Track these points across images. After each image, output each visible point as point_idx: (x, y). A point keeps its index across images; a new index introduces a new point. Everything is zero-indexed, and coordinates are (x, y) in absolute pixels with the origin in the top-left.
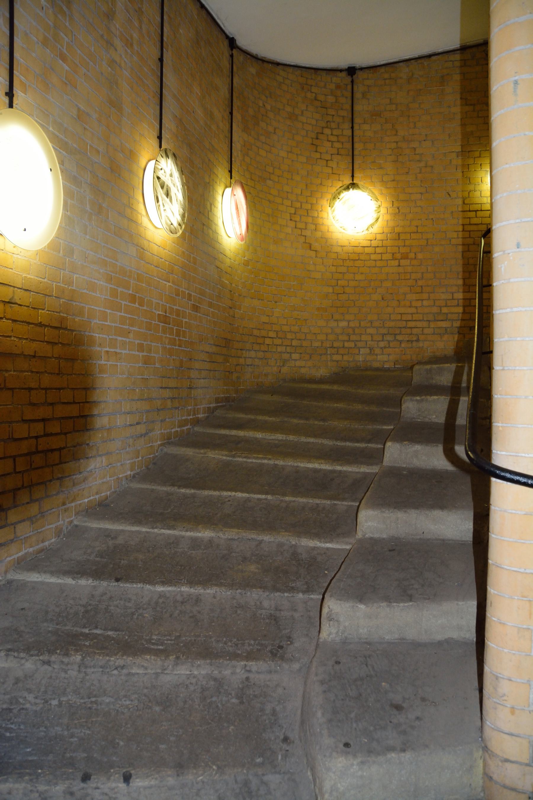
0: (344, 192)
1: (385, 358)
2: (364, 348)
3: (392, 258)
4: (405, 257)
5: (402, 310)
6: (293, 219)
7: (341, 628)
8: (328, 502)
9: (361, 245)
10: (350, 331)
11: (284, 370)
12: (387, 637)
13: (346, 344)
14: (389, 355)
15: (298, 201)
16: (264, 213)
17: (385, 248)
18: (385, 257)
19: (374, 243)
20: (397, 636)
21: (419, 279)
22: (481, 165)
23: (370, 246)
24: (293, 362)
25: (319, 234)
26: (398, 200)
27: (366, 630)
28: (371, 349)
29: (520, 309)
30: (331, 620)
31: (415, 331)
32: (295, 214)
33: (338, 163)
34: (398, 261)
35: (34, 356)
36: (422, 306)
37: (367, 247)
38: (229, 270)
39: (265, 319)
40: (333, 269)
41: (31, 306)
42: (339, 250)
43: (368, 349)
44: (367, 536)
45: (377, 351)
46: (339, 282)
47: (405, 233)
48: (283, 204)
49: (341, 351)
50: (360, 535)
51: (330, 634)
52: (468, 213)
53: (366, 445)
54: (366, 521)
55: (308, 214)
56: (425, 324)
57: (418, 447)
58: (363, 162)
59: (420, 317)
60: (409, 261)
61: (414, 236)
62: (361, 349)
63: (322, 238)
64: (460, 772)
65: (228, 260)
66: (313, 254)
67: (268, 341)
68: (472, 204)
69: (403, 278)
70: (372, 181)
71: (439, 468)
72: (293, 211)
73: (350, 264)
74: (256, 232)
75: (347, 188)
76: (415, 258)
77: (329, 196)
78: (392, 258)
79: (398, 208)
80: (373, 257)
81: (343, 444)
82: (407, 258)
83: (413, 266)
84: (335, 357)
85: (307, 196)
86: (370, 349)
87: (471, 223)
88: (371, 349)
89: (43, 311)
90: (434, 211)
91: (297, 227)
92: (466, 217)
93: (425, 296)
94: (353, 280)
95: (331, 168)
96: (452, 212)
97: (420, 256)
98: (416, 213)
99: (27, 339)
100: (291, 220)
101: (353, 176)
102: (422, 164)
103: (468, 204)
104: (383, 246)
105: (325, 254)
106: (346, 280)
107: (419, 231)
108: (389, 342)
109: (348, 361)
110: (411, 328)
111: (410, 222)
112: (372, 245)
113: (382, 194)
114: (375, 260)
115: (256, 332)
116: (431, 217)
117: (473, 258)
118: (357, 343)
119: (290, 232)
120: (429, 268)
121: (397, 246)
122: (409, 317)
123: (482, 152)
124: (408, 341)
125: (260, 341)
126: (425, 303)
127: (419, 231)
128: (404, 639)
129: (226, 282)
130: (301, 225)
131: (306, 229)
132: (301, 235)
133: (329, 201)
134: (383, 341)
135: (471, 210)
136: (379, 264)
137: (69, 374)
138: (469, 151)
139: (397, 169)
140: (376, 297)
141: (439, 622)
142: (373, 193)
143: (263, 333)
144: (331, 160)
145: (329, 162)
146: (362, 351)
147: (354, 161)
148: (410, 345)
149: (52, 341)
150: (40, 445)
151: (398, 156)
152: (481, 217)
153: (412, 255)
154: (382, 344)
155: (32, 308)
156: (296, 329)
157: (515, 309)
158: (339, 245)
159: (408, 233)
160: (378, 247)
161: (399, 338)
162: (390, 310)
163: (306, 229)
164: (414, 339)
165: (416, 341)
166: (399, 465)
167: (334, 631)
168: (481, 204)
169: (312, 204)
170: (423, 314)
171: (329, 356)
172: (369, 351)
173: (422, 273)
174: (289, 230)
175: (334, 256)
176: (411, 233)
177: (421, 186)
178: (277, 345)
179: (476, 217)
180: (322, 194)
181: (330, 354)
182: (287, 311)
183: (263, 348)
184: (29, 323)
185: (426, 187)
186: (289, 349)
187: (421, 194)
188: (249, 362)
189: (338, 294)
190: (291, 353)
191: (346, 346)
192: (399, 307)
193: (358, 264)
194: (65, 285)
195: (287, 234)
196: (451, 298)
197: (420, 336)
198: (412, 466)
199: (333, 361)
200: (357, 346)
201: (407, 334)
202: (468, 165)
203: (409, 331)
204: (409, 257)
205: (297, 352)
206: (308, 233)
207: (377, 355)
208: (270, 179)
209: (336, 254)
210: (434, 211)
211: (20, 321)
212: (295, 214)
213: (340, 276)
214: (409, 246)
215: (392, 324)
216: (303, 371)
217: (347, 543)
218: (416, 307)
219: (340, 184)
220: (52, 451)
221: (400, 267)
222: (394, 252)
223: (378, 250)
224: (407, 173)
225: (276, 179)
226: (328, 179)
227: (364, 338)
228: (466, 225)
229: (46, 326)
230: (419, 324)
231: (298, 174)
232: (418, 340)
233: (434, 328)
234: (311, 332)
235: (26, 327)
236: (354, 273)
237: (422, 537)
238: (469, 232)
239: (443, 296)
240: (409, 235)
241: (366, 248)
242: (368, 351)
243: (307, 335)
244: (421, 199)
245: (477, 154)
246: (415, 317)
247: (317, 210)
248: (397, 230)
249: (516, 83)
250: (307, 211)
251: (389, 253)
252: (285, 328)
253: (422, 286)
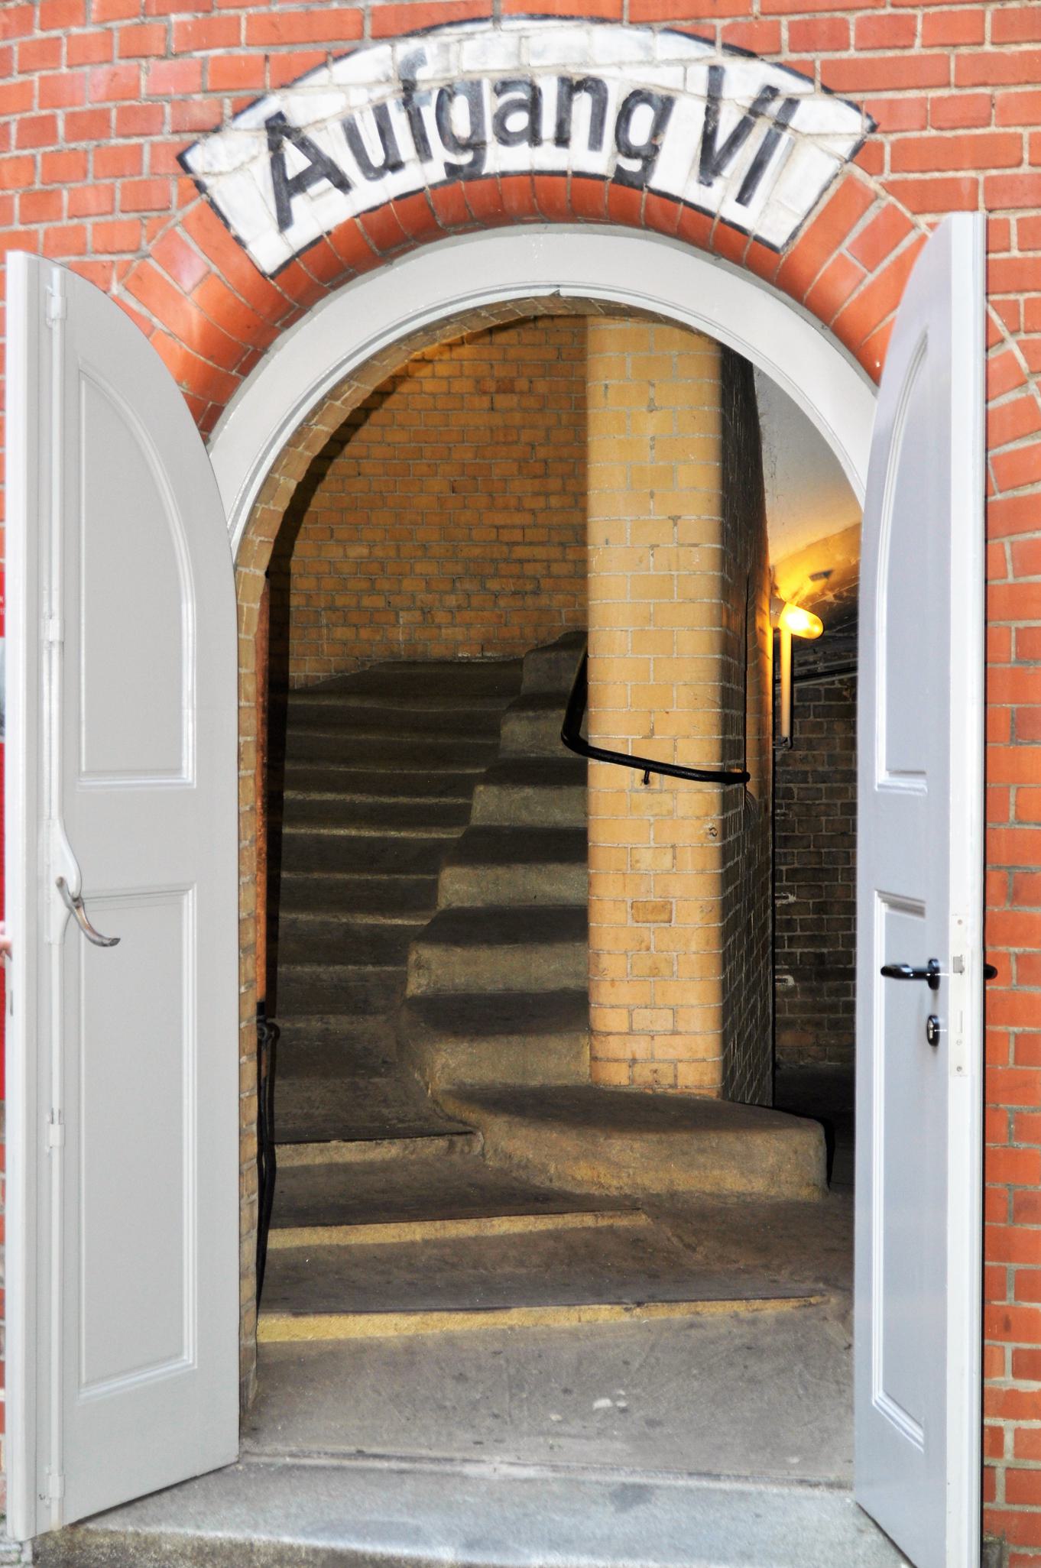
1: (459, 633)
4: (506, 387)
5: (500, 519)
7: (433, 978)
8: (385, 877)
12: (491, 988)
13: (366, 602)
14: (469, 626)
18: (458, 386)
20: (501, 986)
27: (463, 980)
28: (427, 612)
29: (608, 601)
30: (420, 969)
36: (548, 508)
43: (418, 613)
44: (454, 905)
45: (441, 617)
50: (442, 903)
51: (419, 986)
53: (437, 800)
54: (452, 883)
57: (529, 791)
60: (515, 398)
62: (401, 614)
64: (568, 1059)
71: (565, 825)
76: (530, 390)
81: (393, 800)
84: (341, 633)
88: (427, 612)
97: (541, 387)
110: (521, 561)
122: (517, 536)
128: (509, 990)
134: (453, 591)
140: (437, 485)
141: (552, 967)
146: (404, 617)
153: (522, 384)
154: (452, 601)
157: (604, 601)
161: (493, 585)
164: (529, 587)
166: (496, 824)
167: (424, 982)
171: (325, 631)
172: (421, 618)
197: (542, 581)
198: (520, 824)
204: (517, 389)
217: (424, 918)
218: (533, 512)
230: (540, 552)
232: (536, 593)
233: (574, 562)
237: (533, 903)
249: (606, 387)
251: (467, 377)
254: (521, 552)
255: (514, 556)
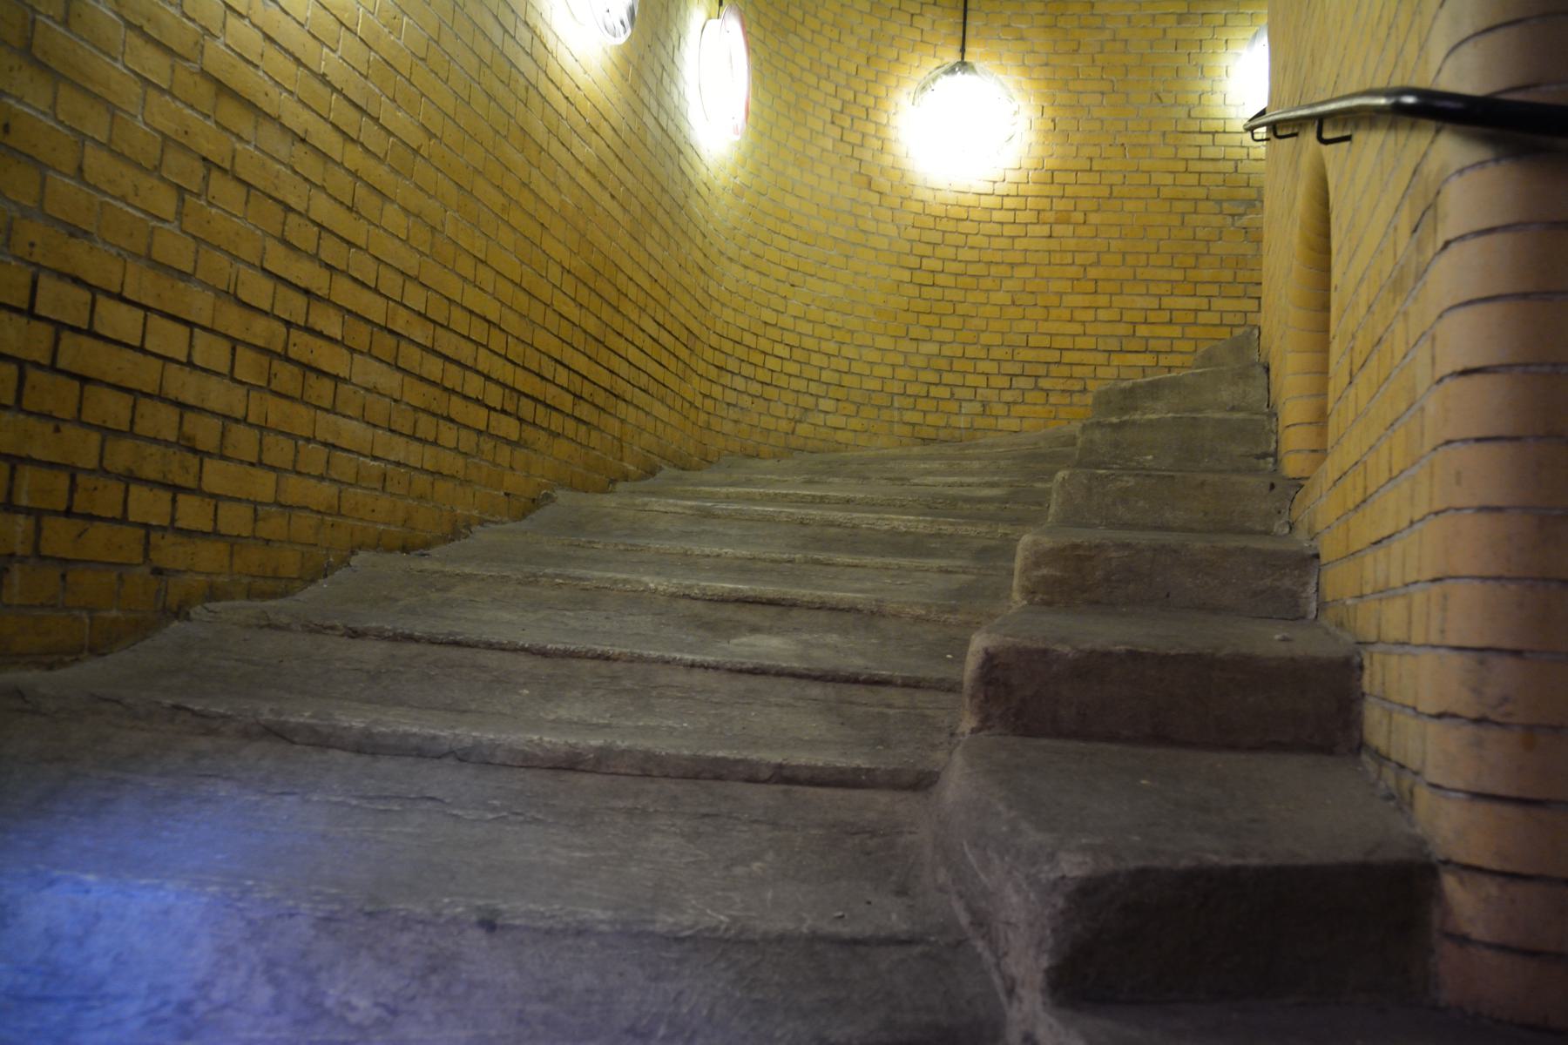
0: (944, 77)
2: (971, 400)
3: (1036, 221)
5: (1052, 327)
6: (837, 122)
9: (973, 190)
10: (943, 364)
11: (802, 429)
13: (934, 391)
15: (848, 86)
16: (780, 97)
17: (1024, 199)
18: (1021, 217)
19: (1001, 189)
21: (1090, 265)
22: (1226, 41)
23: (993, 194)
24: (822, 415)
25: (887, 160)
26: (1053, 105)
31: (1077, 371)
32: (842, 112)
33: (934, 22)
34: (1049, 226)
35: (303, 140)
37: (986, 194)
38: (703, 190)
39: (769, 316)
40: (914, 234)
41: (307, 28)
42: (927, 195)
45: (999, 409)
46: (925, 261)
47: (1066, 170)
48: (818, 88)
49: (923, 404)
52: (1198, 137)
55: (867, 115)
56: (1101, 358)
58: (986, 25)
59: (1091, 343)
60: (1071, 228)
61: (1083, 178)
62: (964, 404)
63: (893, 167)
65: (703, 170)
66: (874, 198)
67: (772, 363)
68: (1208, 119)
69: (1058, 262)
70: (1002, 64)
72: (838, 106)
73: (951, 226)
74: (762, 134)
75: (952, 71)
76: (1085, 223)
77: (912, 86)
78: (1036, 221)
79: (1053, 120)
80: (997, 216)
82: (1068, 222)
83: (1079, 237)
84: (911, 416)
85: (867, 81)
86: (984, 406)
87: (1203, 156)
89: (332, 54)
90: (1126, 130)
91: (844, 138)
92: (1194, 143)
93: (1103, 300)
94: (954, 260)
95: (919, 32)
96: (1164, 134)
97: (1094, 218)
98: (1090, 131)
99: (291, 93)
100: (833, 123)
101: (963, 50)
102: (1107, 35)
103: (1196, 118)
104: (1017, 196)
105: (899, 201)
106: (939, 259)
107: (1095, 167)
108: (1023, 391)
109: (937, 427)
111: (1077, 148)
112: (996, 192)
113: (1021, 89)
114: (1002, 223)
115: (748, 339)
116: (1120, 140)
117: (1204, 227)
118: (956, 390)
119: (830, 147)
120: (1113, 243)
121: (1047, 197)
122: (1068, 343)
123: (1229, 17)
124: (1063, 391)
125: (757, 358)
126: (1102, 314)
127: (1095, 167)
129: (697, 210)
130: (854, 138)
131: (862, 146)
132: (852, 157)
133: (912, 95)
135: (1203, 130)
136: (1008, 230)
137: (374, 224)
138: (1203, 14)
139: (1055, 42)
142: (1002, 84)
143: (764, 345)
144: (921, 14)
145: (915, 17)
147: (968, 21)
148: (1068, 401)
149: (345, 129)
150: (295, 345)
151: (1056, 17)
152: (1225, 146)
155: (309, 32)
156: (831, 347)
158: (929, 185)
159: (1072, 171)
160: (1008, 195)
162: (1027, 326)
163: (862, 146)
164: (1078, 386)
165: (1080, 391)
168: (1225, 119)
169: (876, 98)
170: (1097, 336)
173: (1098, 253)
174: (829, 144)
175: (917, 207)
176: (1077, 172)
177: (1102, 79)
178: (790, 375)
179: (1214, 145)
180: (898, 81)
181: (899, 409)
182: (812, 307)
183: (762, 375)
184: (298, 62)
185: (1112, 81)
186: (813, 388)
187: (1103, 93)
188: (731, 397)
189: (921, 285)
190: (818, 396)
191: (932, 394)
192: (1046, 320)
193: (964, 227)
194: (385, 26)
195: (823, 150)
196: (1157, 307)
197: (1088, 382)
199: (905, 423)
200: (956, 397)
201: (1063, 377)
202: (1201, 41)
203: (1065, 371)
205: (831, 395)
206: (867, 155)
207: (997, 417)
208: (795, 33)
209: (922, 204)
210: (1126, 130)
211: (280, 46)
212: (842, 112)
213: (928, 250)
214: (1073, 198)
215: (1029, 355)
216: (840, 436)
218: (1083, 323)
219: (937, 63)
220: (321, 373)
221: (1053, 240)
222: (1040, 207)
223: (1009, 203)
224: (1077, 50)
225: (808, 36)
226: (912, 51)
227: (971, 380)
228: (1193, 159)
229: (334, 89)
231: (852, 33)
234: (861, 357)
235: (291, 67)
236: (957, 247)
238: (1197, 176)
239: (1141, 302)
240: (1074, 174)
241: (982, 197)
242: (977, 407)
243: (853, 363)
244: (1101, 105)
245: (1219, 20)
246: (1081, 342)
247: (886, 112)
248: (1049, 164)
250: (867, 110)
251: (1031, 210)
252: (810, 343)
253: (1096, 281)
254: (1069, 357)
255: (1065, 360)
